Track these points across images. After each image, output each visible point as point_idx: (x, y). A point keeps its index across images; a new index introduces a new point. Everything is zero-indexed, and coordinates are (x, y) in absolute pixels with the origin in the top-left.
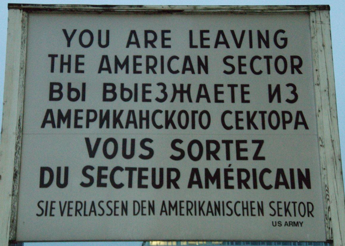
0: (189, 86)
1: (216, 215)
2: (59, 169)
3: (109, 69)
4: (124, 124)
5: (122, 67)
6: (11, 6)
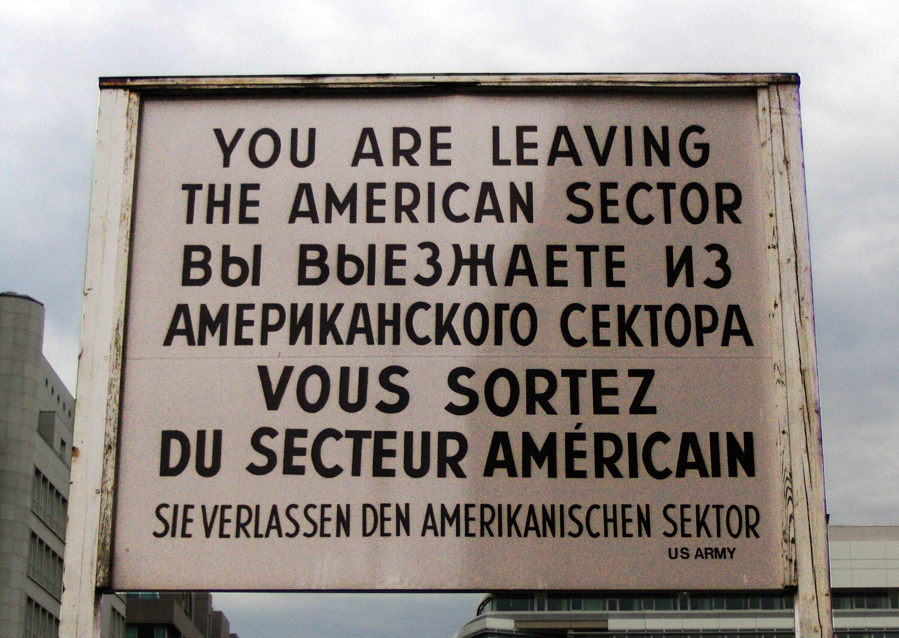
0: (490, 248)
1: (545, 535)
2: (201, 435)
3: (312, 214)
4: (344, 337)
6: (107, 83)
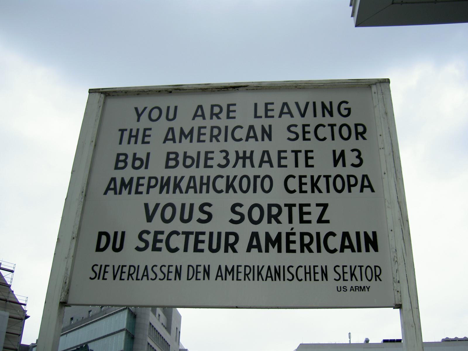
0: (252, 152)
1: (275, 280)
2: (116, 233)
4: (184, 190)
5: (186, 137)
6: (91, 91)
